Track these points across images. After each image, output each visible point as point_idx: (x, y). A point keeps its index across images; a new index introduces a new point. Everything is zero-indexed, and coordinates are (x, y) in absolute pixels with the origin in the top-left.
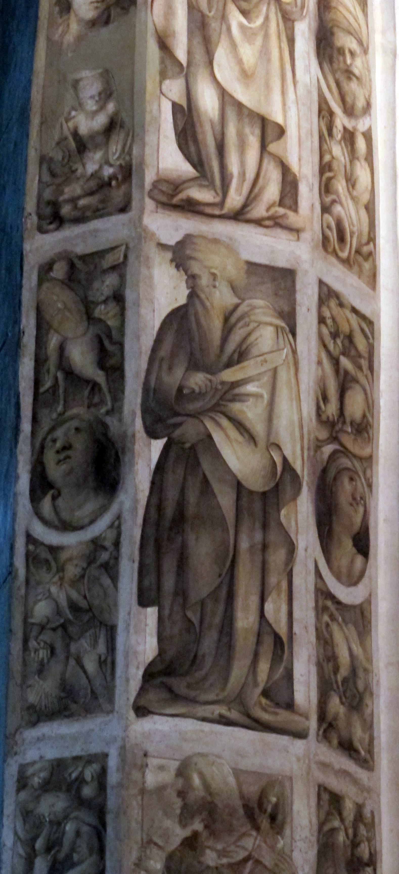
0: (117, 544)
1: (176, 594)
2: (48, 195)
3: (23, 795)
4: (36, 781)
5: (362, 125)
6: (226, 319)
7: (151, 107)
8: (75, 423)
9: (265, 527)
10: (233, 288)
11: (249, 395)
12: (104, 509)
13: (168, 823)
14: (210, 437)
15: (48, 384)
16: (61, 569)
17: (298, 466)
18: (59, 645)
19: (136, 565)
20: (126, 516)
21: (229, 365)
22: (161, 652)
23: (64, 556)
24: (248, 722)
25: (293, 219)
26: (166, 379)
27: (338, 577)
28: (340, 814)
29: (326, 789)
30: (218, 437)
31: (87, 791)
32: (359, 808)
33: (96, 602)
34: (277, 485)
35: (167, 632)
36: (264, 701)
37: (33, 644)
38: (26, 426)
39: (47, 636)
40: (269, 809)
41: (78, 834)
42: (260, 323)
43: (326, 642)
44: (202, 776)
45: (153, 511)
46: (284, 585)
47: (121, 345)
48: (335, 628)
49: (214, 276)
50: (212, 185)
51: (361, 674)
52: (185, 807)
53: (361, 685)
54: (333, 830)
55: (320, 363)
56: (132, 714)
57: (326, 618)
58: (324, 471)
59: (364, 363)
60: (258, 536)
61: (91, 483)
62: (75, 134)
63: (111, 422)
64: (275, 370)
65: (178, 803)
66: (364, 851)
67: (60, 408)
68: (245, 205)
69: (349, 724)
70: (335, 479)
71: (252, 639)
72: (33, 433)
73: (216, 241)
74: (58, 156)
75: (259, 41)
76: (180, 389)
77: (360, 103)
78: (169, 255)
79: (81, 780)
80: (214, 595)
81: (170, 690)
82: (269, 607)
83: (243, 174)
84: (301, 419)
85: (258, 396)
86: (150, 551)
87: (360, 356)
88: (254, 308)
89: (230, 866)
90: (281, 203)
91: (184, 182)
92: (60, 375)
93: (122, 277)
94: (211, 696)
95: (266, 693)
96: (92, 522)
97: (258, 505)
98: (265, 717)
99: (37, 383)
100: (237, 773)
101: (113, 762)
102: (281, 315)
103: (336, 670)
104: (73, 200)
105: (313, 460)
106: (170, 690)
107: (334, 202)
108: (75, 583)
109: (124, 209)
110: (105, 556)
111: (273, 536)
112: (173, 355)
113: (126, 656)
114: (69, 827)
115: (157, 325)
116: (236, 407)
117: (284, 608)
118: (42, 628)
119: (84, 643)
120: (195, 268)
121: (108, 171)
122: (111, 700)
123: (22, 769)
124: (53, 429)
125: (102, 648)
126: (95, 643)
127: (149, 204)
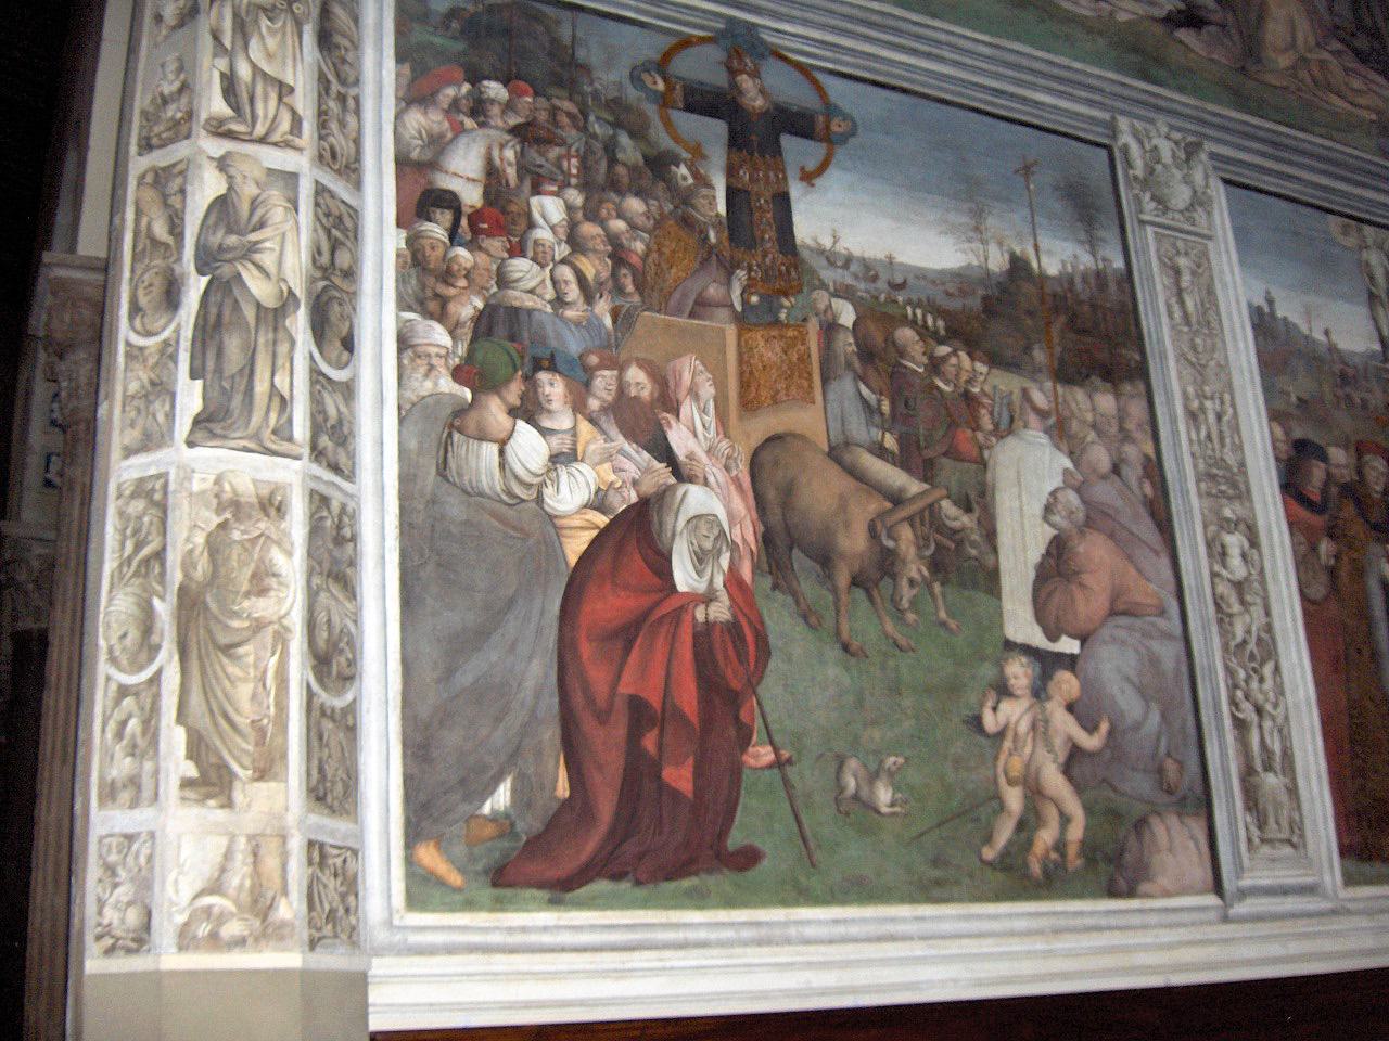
0: (178, 342)
1: (215, 371)
2: (144, 133)
3: (120, 502)
4: (127, 493)
5: (352, 92)
6: (252, 203)
7: (205, 77)
8: (155, 270)
9: (275, 329)
10: (258, 184)
11: (266, 249)
12: (170, 321)
13: (207, 514)
14: (239, 275)
15: (140, 248)
16: (145, 361)
17: (298, 292)
18: (142, 407)
19: (188, 354)
20: (183, 323)
21: (253, 230)
22: (205, 407)
23: (147, 352)
24: (261, 449)
25: (298, 142)
26: (211, 239)
27: (329, 363)
28: (328, 508)
29: (317, 492)
30: (245, 275)
31: (157, 496)
32: (343, 508)
33: (165, 379)
34: (284, 305)
35: (210, 395)
36: (273, 437)
37: (127, 408)
38: (127, 274)
39: (136, 403)
40: (276, 503)
41: (151, 523)
42: (275, 205)
43: (318, 402)
44: (230, 483)
45: (200, 320)
46: (288, 365)
47: (183, 219)
48: (326, 395)
49: (245, 177)
50: (245, 121)
51: (345, 422)
52: (219, 504)
53: (346, 430)
54: (322, 519)
55: (315, 230)
56: (184, 446)
57: (318, 387)
58: (318, 297)
59: (351, 234)
60: (271, 336)
61: (165, 305)
62: (162, 95)
63: (177, 268)
64: (284, 234)
65: (215, 501)
66: (347, 532)
67: (147, 261)
68: (267, 134)
69: (335, 453)
70: (327, 303)
71: (266, 400)
72: (131, 279)
73: (247, 156)
74: (151, 109)
75: (279, 36)
76: (221, 245)
77: (351, 79)
78: (215, 164)
79: (153, 490)
80: (241, 370)
81: (211, 432)
82: (277, 379)
83: (266, 117)
84: (300, 263)
85: (272, 250)
86: (199, 344)
87: (347, 230)
88: (269, 196)
89: (249, 540)
90: (291, 133)
91: (226, 119)
92: (148, 242)
93: (185, 177)
94: (238, 434)
95: (274, 432)
96: (164, 329)
97: (271, 316)
98: (274, 447)
99: (135, 247)
100: (255, 482)
101: (172, 477)
102: (289, 200)
103: (326, 420)
104: (159, 135)
105: (309, 292)
106: (211, 432)
107: (328, 135)
108: (152, 368)
109: (188, 137)
110: (170, 350)
111: (281, 335)
112: (216, 225)
113: (182, 410)
114: (146, 520)
115: (206, 207)
116: (257, 257)
117: (288, 380)
118: (133, 397)
119: (157, 405)
120: (232, 171)
121: (179, 115)
122: (172, 439)
123: (119, 487)
124: (143, 274)
125: (167, 407)
126: (163, 406)
127: (203, 133)
